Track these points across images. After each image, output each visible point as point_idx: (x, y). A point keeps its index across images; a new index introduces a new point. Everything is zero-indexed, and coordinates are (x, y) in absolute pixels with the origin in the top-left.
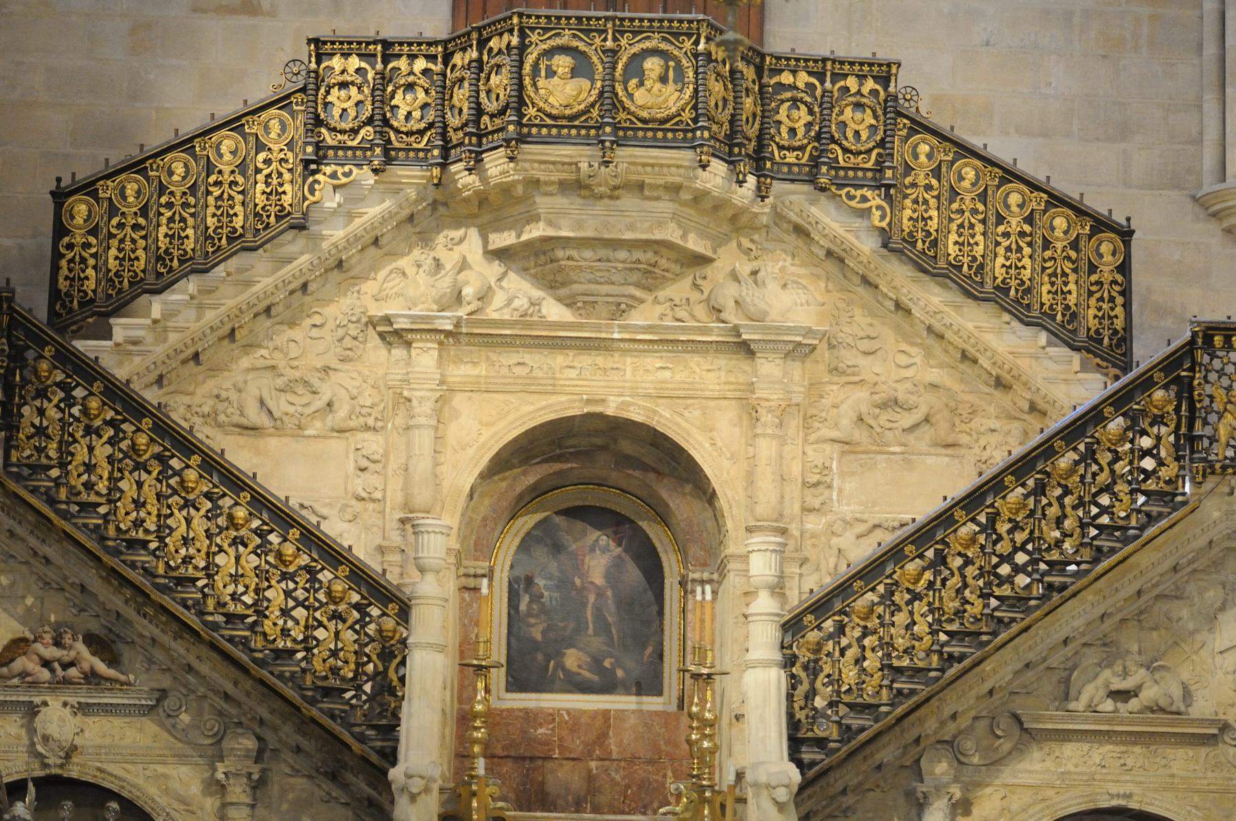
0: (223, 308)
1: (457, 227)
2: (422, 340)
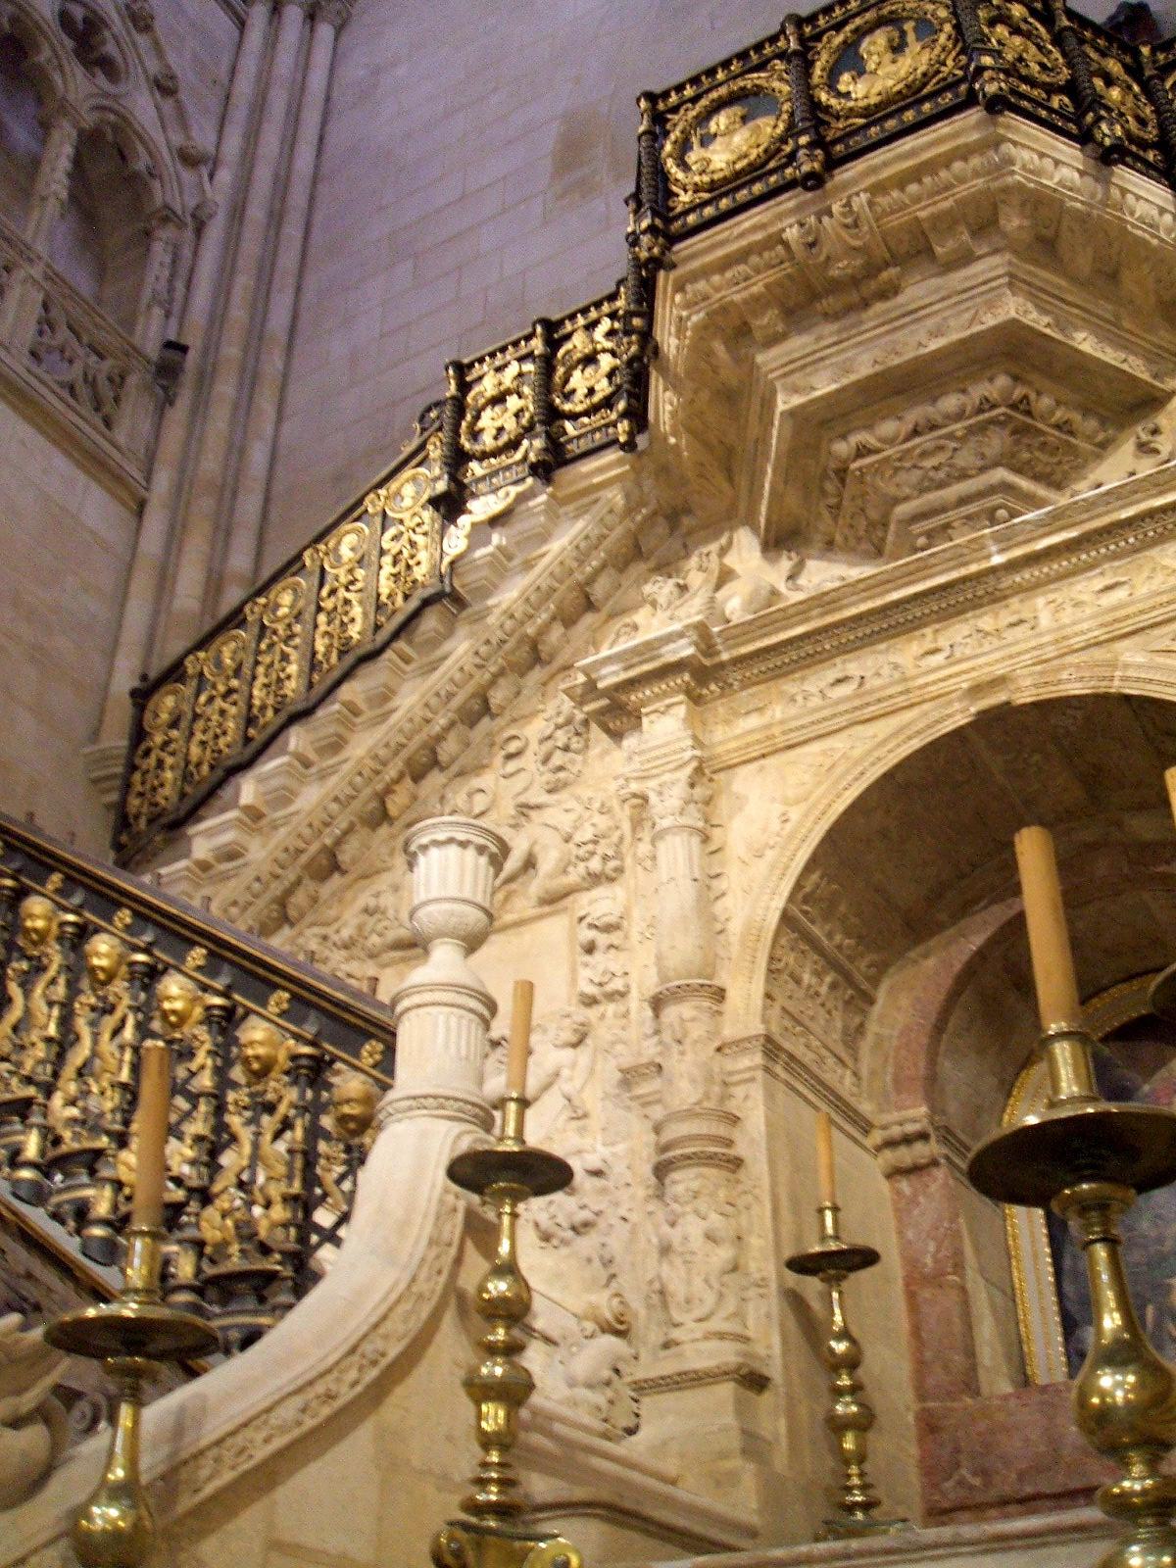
0: (346, 767)
1: (716, 536)
2: (658, 697)
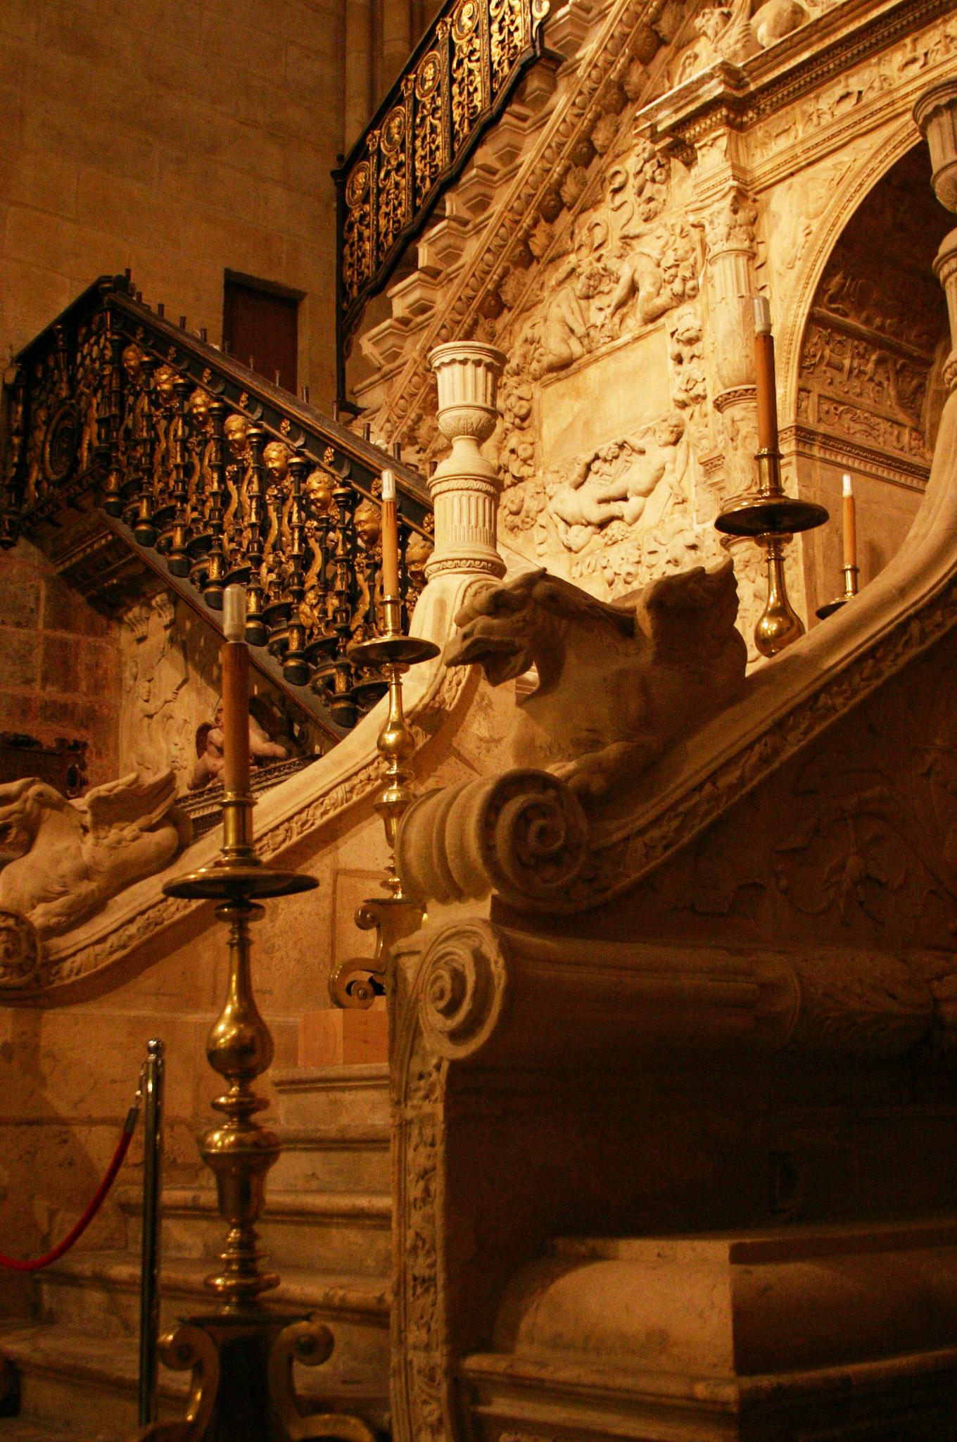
2: (706, 131)
